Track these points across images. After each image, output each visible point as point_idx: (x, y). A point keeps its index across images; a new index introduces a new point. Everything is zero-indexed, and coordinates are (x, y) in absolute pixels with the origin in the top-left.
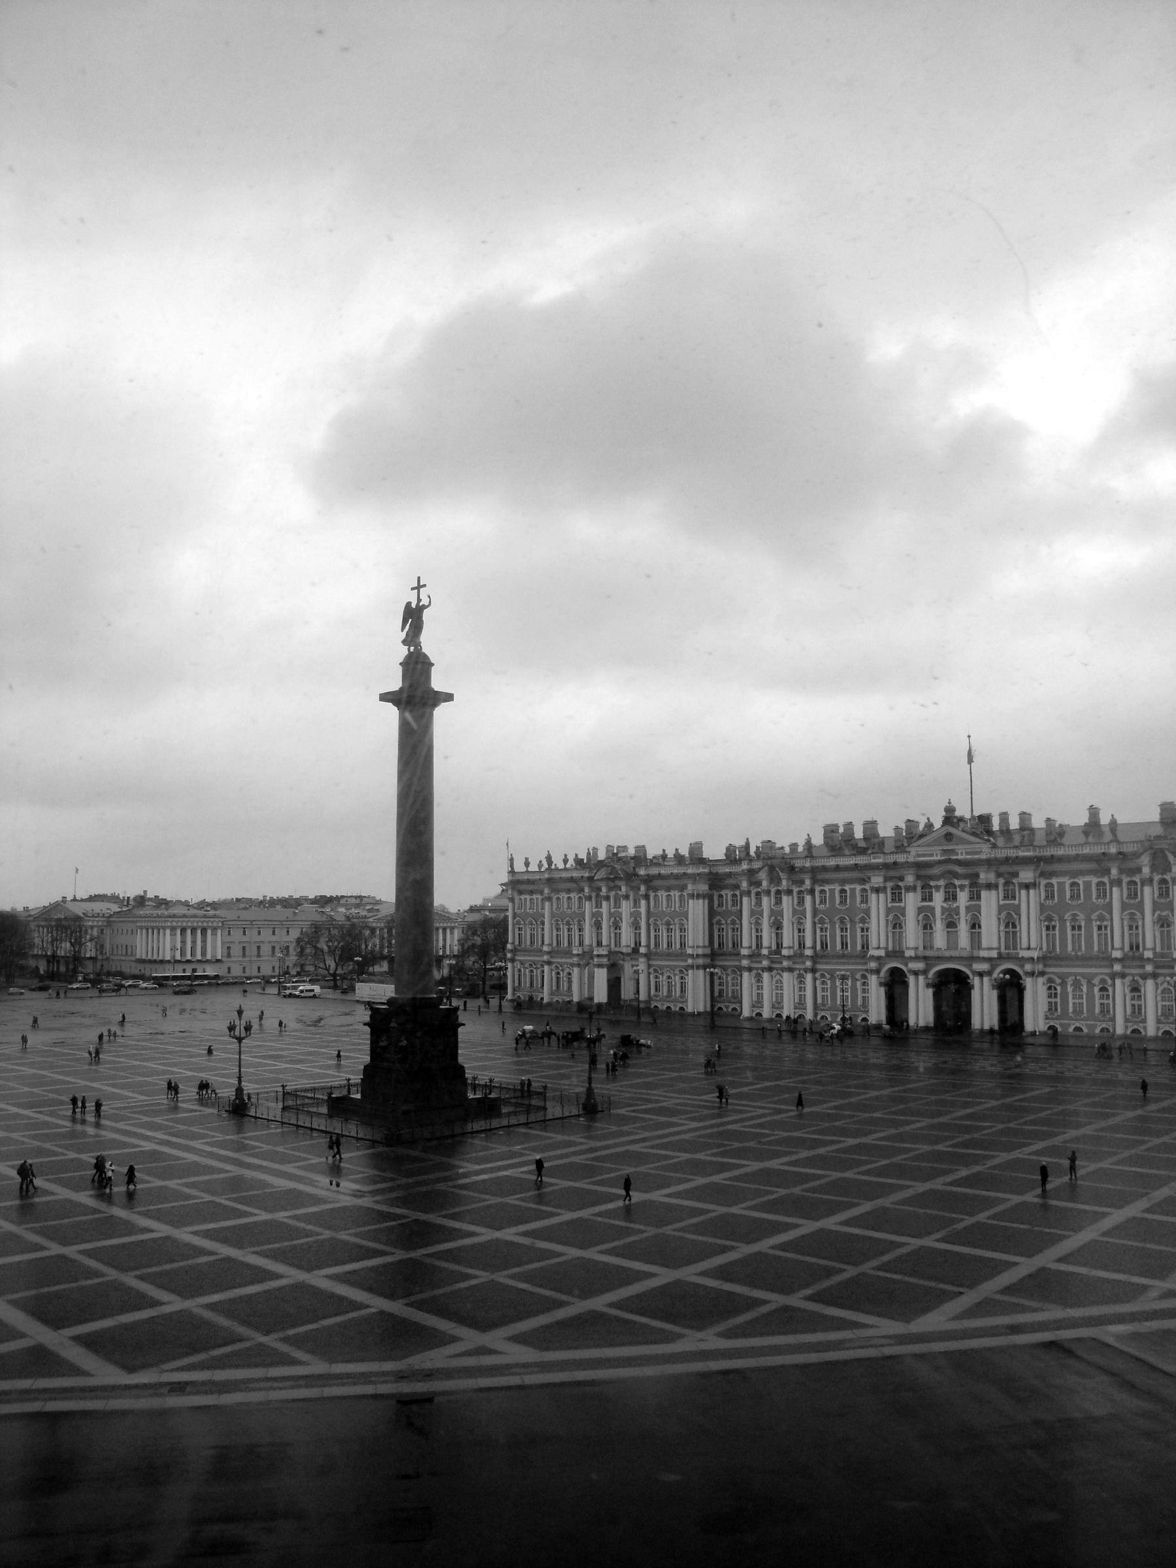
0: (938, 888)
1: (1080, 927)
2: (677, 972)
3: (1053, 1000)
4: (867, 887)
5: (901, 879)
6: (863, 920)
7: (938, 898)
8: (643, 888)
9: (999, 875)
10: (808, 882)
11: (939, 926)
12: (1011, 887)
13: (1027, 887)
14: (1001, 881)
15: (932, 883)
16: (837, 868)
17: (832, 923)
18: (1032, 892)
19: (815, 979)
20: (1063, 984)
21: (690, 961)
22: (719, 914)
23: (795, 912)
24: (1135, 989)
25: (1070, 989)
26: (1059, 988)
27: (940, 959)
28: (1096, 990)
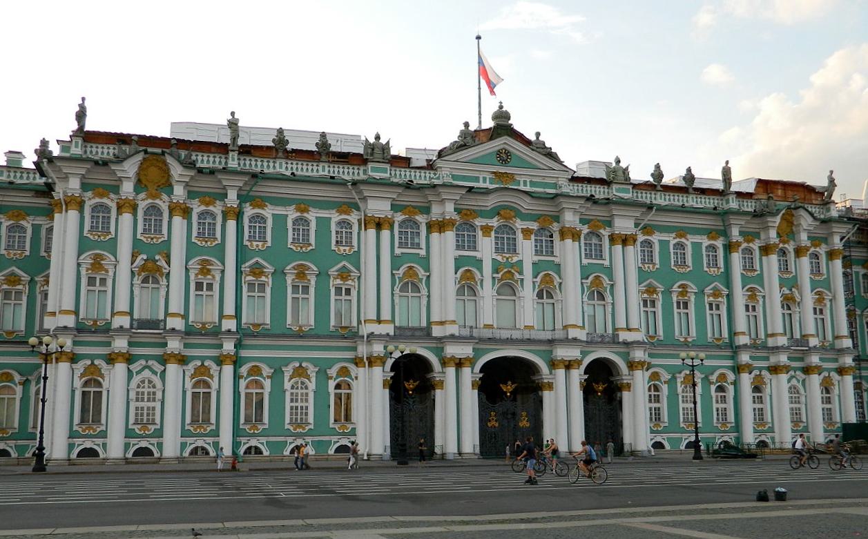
0: (486, 230)
1: (686, 305)
3: (654, 405)
4: (353, 218)
5: (426, 210)
6: (344, 274)
7: (486, 248)
10: (232, 195)
11: (487, 291)
12: (594, 241)
13: (626, 240)
15: (479, 222)
16: (293, 179)
17: (279, 274)
18: (630, 248)
19: (237, 377)
20: (672, 382)
23: (191, 250)
25: (680, 389)
26: (665, 389)
28: (713, 388)
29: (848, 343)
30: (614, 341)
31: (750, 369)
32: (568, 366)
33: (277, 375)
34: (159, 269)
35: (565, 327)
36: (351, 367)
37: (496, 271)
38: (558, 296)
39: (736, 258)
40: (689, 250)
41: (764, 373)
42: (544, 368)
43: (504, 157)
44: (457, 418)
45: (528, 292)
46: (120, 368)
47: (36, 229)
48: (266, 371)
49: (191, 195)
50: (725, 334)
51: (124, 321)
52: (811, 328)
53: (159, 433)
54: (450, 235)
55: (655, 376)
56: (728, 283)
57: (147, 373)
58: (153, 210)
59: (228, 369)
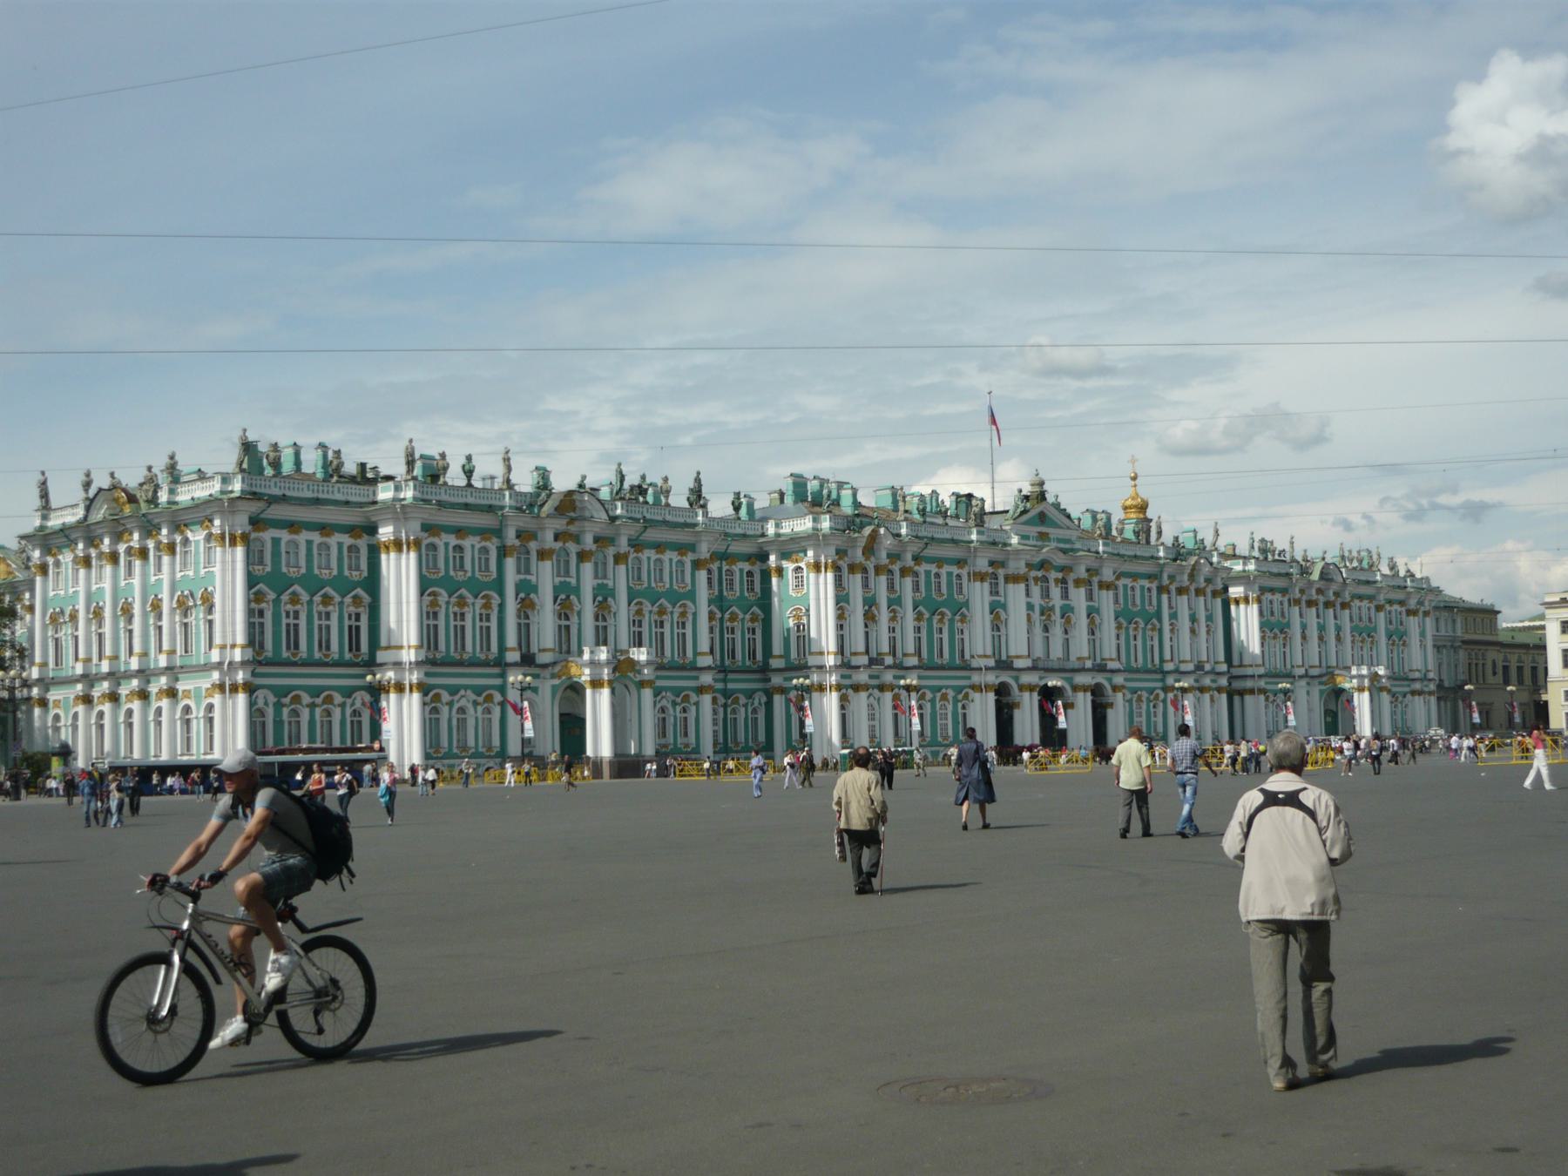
4: (964, 572)
5: (1003, 564)
11: (1038, 630)
15: (1033, 574)
30: (1101, 668)
32: (1085, 689)
35: (1079, 659)
37: (1042, 614)
39: (1165, 597)
43: (1042, 518)
45: (1057, 630)
46: (863, 695)
48: (929, 695)
50: (1157, 661)
54: (1022, 586)
56: (1160, 620)
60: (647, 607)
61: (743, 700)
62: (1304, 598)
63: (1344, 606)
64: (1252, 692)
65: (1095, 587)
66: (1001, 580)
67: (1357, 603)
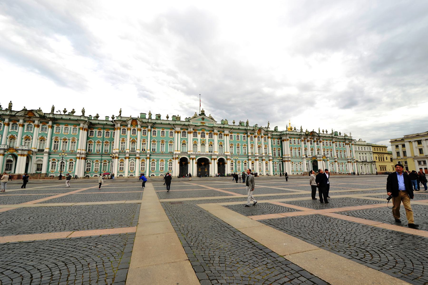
0: (199, 133)
1: (239, 147)
2: (68, 160)
4: (173, 131)
5: (187, 129)
7: (199, 136)
8: (50, 123)
9: (218, 131)
11: (199, 145)
14: (219, 133)
15: (198, 132)
18: (228, 137)
19: (150, 161)
21: (78, 155)
22: (91, 138)
24: (253, 164)
25: (237, 164)
26: (234, 164)
27: (200, 155)
29: (271, 155)
31: (251, 160)
32: (214, 159)
33: (158, 161)
34: (135, 141)
36: (172, 160)
38: (213, 146)
39: (249, 138)
40: (240, 137)
41: (254, 161)
42: (210, 160)
43: (203, 119)
44: (193, 168)
45: (207, 145)
46: (127, 160)
47: (111, 132)
48: (155, 160)
49: (142, 127)
51: (128, 151)
52: (264, 152)
53: (135, 172)
54: (192, 134)
55: (232, 161)
57: (132, 161)
58: (134, 130)
59: (148, 160)
60: (59, 138)
61: (107, 161)
62: (306, 140)
63: (320, 142)
64: (287, 161)
65: (223, 135)
66: (187, 133)
67: (325, 142)
